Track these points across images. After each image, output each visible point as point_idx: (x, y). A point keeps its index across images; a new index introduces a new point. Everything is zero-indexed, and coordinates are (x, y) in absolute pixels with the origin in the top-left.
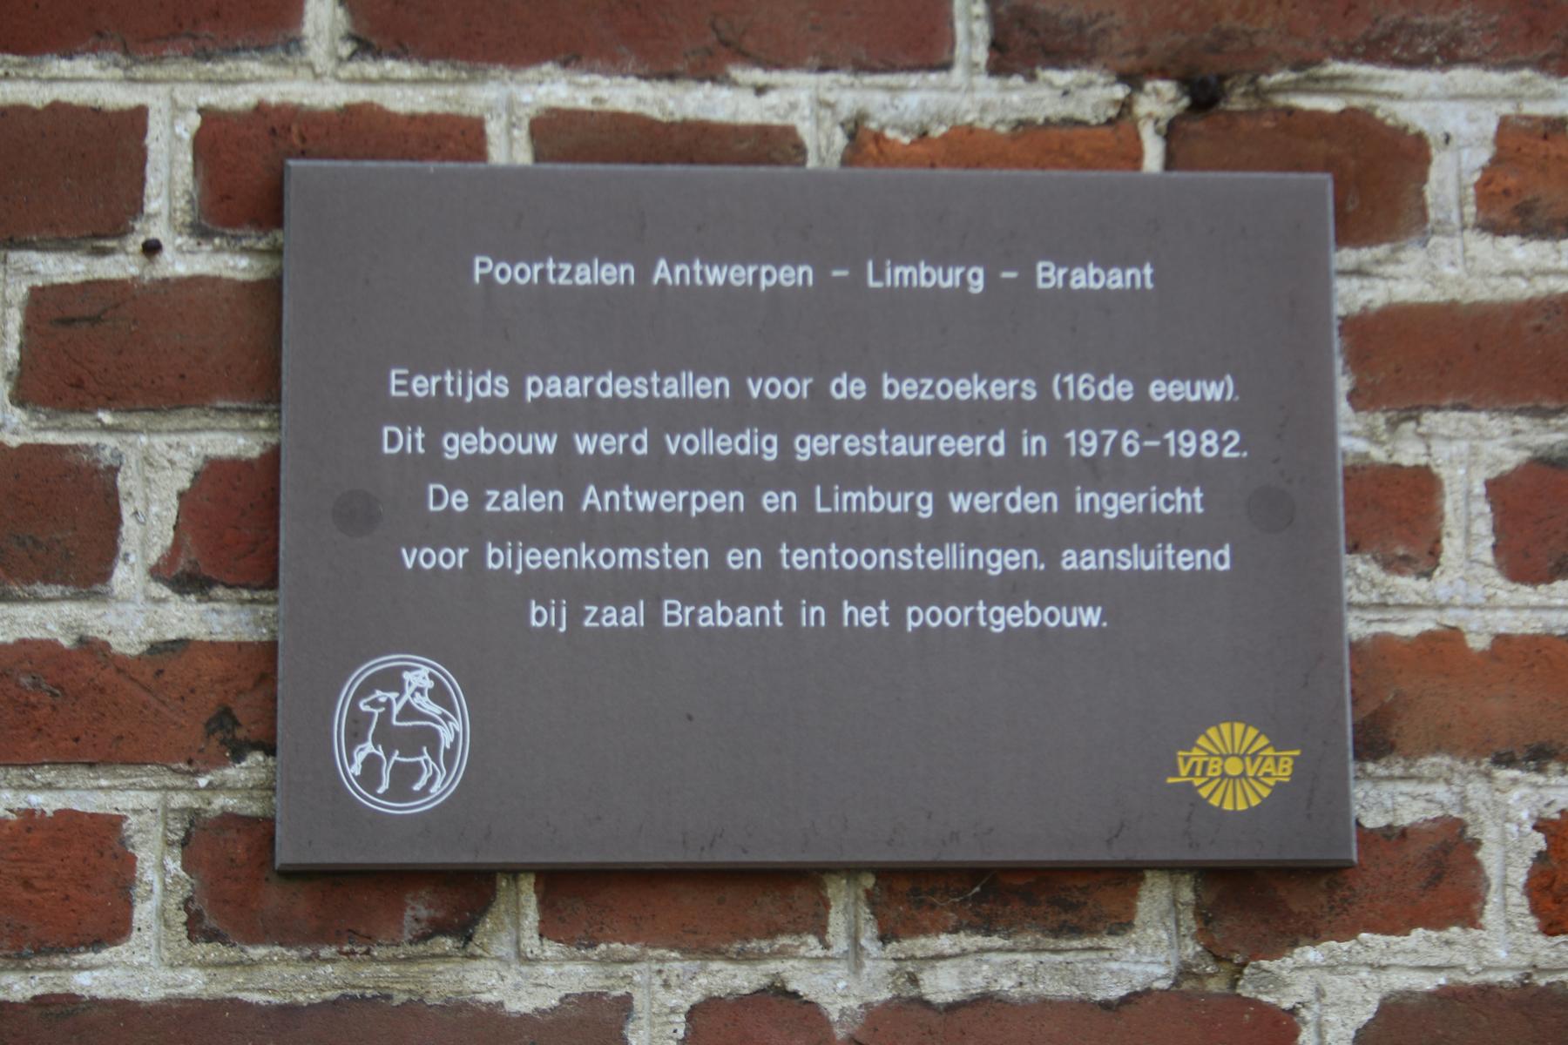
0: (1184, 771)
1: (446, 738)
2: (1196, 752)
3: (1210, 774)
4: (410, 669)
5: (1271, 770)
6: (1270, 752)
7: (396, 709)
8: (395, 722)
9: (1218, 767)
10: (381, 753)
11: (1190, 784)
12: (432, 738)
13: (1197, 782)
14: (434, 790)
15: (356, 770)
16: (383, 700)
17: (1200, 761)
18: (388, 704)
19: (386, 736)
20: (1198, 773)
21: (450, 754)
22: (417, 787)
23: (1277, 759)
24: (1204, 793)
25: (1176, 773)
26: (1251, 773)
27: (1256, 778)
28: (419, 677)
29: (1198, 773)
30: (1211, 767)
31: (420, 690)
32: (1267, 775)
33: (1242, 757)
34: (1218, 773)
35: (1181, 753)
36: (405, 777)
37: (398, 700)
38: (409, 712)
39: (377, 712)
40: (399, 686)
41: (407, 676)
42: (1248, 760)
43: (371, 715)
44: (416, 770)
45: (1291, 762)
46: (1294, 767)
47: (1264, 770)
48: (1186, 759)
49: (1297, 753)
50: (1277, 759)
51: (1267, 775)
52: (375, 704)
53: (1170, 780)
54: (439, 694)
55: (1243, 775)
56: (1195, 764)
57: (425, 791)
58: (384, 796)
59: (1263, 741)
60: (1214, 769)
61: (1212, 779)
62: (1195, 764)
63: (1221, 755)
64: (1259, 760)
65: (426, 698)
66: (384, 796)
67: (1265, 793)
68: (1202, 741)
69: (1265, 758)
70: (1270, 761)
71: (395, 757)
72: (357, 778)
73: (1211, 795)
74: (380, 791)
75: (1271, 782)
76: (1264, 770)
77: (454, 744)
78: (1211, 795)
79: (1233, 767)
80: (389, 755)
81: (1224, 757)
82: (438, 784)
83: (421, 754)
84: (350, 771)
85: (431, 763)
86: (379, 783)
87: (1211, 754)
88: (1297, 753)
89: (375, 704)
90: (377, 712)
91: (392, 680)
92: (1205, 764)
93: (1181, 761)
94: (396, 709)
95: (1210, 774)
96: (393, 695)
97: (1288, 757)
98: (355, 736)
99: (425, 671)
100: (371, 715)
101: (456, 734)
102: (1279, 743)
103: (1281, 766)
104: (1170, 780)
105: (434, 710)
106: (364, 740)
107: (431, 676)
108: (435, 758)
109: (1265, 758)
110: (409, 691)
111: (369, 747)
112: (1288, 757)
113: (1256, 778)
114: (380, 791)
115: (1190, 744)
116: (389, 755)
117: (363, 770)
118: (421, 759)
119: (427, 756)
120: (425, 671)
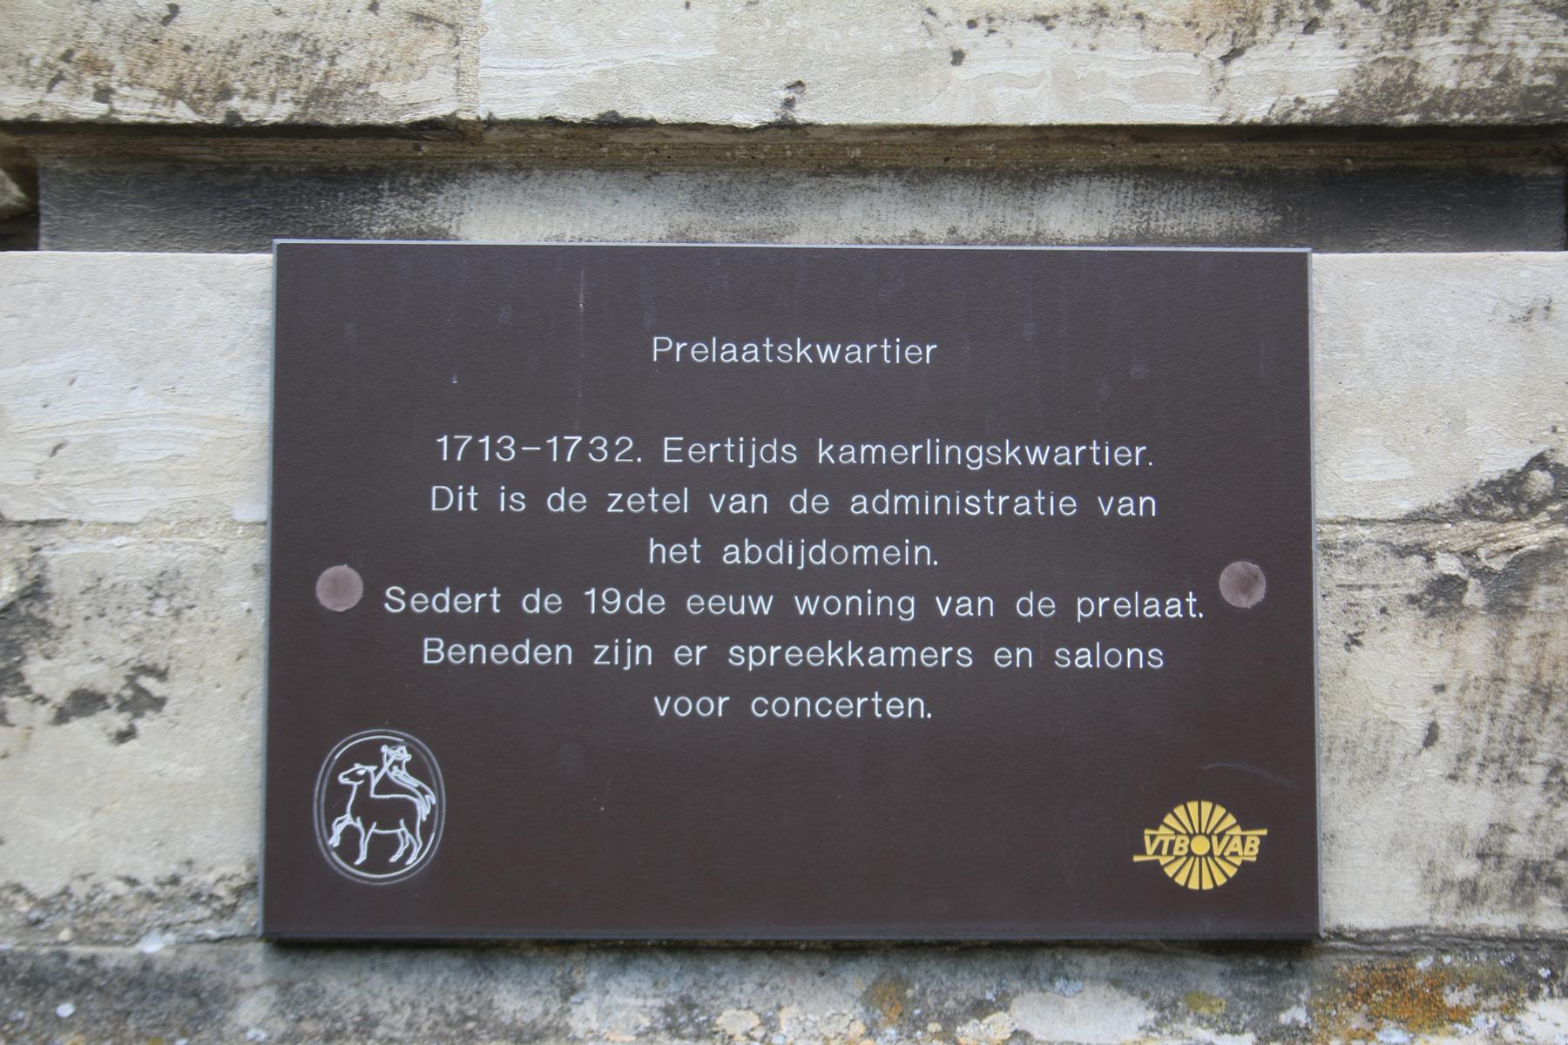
0: (1150, 849)
1: (423, 811)
2: (1163, 830)
5: (1239, 849)
6: (1237, 831)
7: (374, 782)
8: (372, 795)
10: (359, 824)
11: (1157, 862)
12: (409, 811)
14: (412, 861)
15: (335, 841)
16: (361, 773)
18: (367, 776)
19: (365, 809)
20: (1165, 851)
21: (426, 829)
22: (393, 859)
23: (1243, 839)
24: (1170, 871)
25: (1144, 853)
26: (1217, 852)
27: (1222, 857)
29: (1165, 851)
30: (1177, 845)
31: (398, 763)
32: (1234, 854)
33: (1209, 837)
34: (1185, 851)
35: (1148, 832)
36: (380, 848)
37: (376, 772)
38: (386, 785)
39: (356, 784)
40: (377, 760)
41: (384, 749)
42: (1214, 839)
43: (350, 788)
44: (393, 843)
45: (1258, 842)
46: (1260, 847)
47: (1231, 849)
48: (1153, 838)
49: (1264, 832)
50: (1243, 839)
51: (1234, 854)
52: (354, 776)
53: (1137, 859)
54: (415, 769)
55: (1210, 853)
56: (1161, 843)
57: (401, 863)
58: (358, 867)
59: (1231, 820)
60: (1181, 844)
61: (1178, 858)
62: (1161, 843)
63: (1188, 834)
64: (1226, 839)
65: (404, 771)
66: (362, 867)
67: (1232, 872)
68: (1169, 819)
70: (1237, 840)
71: (373, 829)
72: (337, 850)
73: (1176, 874)
74: (358, 862)
75: (1238, 861)
76: (1231, 849)
78: (1176, 874)
80: (367, 828)
81: (1191, 837)
85: (408, 835)
86: (357, 856)
87: (1177, 833)
88: (1264, 832)
89: (354, 776)
90: (356, 784)
91: (371, 754)
92: (1172, 844)
93: (1147, 840)
94: (374, 782)
95: (1176, 852)
97: (1255, 837)
98: (335, 811)
100: (350, 788)
101: (433, 807)
102: (1246, 823)
103: (1248, 844)
104: (1137, 859)
105: (412, 783)
106: (344, 813)
108: (412, 831)
110: (387, 765)
111: (348, 819)
112: (1255, 837)
113: (1222, 857)
114: (358, 862)
115: (1156, 823)
116: (367, 828)
117: (342, 841)
118: (398, 831)
119: (404, 828)
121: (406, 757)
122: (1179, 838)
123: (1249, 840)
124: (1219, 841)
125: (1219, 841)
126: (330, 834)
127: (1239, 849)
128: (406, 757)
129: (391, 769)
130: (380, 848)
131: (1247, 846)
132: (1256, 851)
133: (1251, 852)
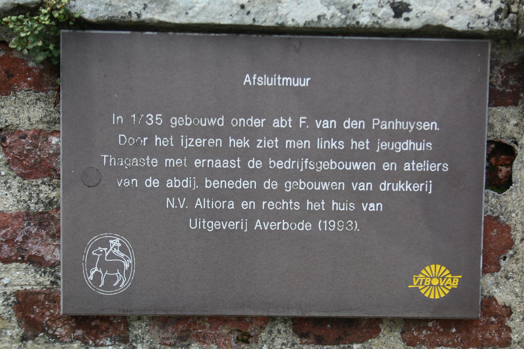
0: (415, 283)
1: (126, 266)
2: (420, 275)
3: (425, 284)
4: (113, 239)
5: (450, 283)
6: (450, 276)
7: (107, 254)
9: (429, 282)
10: (101, 272)
13: (420, 287)
15: (91, 278)
16: (101, 251)
17: (422, 279)
19: (103, 265)
20: (421, 284)
21: (128, 272)
22: (115, 284)
23: (452, 279)
24: (423, 291)
26: (442, 284)
27: (443, 286)
28: (115, 242)
29: (421, 284)
30: (426, 281)
31: (116, 247)
32: (448, 285)
33: (438, 278)
36: (110, 280)
37: (107, 251)
38: (111, 255)
40: (108, 246)
41: (111, 242)
42: (441, 279)
44: (115, 278)
45: (458, 280)
47: (447, 283)
48: (416, 278)
49: (460, 277)
50: (452, 279)
51: (448, 285)
52: (98, 252)
53: (410, 287)
54: (123, 249)
55: (439, 285)
56: (420, 280)
59: (447, 272)
60: (428, 281)
61: (426, 286)
62: (420, 280)
63: (430, 277)
64: (446, 279)
65: (118, 250)
67: (447, 292)
68: (423, 271)
69: (448, 278)
70: (450, 280)
71: (106, 273)
75: (450, 288)
76: (447, 283)
77: (129, 268)
79: (435, 282)
81: (432, 278)
82: (122, 283)
83: (117, 272)
84: (89, 278)
87: (426, 277)
88: (460, 277)
89: (98, 252)
91: (106, 243)
92: (424, 281)
93: (414, 279)
94: (107, 254)
95: (425, 284)
96: (105, 249)
98: (90, 267)
99: (118, 240)
102: (453, 273)
103: (454, 282)
104: (410, 287)
105: (122, 255)
107: (120, 242)
108: (122, 274)
109: (448, 278)
110: (111, 248)
111: (96, 269)
113: (443, 286)
115: (418, 273)
120: (118, 240)
121: (119, 245)
122: (427, 279)
123: (454, 279)
124: (443, 280)
125: (443, 280)
126: (89, 275)
127: (450, 283)
128: (119, 245)
129: (113, 249)
130: (110, 280)
131: (454, 282)
132: (457, 284)
133: (455, 284)
